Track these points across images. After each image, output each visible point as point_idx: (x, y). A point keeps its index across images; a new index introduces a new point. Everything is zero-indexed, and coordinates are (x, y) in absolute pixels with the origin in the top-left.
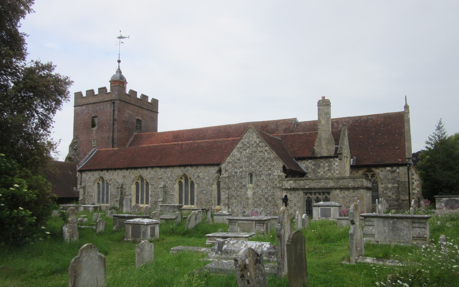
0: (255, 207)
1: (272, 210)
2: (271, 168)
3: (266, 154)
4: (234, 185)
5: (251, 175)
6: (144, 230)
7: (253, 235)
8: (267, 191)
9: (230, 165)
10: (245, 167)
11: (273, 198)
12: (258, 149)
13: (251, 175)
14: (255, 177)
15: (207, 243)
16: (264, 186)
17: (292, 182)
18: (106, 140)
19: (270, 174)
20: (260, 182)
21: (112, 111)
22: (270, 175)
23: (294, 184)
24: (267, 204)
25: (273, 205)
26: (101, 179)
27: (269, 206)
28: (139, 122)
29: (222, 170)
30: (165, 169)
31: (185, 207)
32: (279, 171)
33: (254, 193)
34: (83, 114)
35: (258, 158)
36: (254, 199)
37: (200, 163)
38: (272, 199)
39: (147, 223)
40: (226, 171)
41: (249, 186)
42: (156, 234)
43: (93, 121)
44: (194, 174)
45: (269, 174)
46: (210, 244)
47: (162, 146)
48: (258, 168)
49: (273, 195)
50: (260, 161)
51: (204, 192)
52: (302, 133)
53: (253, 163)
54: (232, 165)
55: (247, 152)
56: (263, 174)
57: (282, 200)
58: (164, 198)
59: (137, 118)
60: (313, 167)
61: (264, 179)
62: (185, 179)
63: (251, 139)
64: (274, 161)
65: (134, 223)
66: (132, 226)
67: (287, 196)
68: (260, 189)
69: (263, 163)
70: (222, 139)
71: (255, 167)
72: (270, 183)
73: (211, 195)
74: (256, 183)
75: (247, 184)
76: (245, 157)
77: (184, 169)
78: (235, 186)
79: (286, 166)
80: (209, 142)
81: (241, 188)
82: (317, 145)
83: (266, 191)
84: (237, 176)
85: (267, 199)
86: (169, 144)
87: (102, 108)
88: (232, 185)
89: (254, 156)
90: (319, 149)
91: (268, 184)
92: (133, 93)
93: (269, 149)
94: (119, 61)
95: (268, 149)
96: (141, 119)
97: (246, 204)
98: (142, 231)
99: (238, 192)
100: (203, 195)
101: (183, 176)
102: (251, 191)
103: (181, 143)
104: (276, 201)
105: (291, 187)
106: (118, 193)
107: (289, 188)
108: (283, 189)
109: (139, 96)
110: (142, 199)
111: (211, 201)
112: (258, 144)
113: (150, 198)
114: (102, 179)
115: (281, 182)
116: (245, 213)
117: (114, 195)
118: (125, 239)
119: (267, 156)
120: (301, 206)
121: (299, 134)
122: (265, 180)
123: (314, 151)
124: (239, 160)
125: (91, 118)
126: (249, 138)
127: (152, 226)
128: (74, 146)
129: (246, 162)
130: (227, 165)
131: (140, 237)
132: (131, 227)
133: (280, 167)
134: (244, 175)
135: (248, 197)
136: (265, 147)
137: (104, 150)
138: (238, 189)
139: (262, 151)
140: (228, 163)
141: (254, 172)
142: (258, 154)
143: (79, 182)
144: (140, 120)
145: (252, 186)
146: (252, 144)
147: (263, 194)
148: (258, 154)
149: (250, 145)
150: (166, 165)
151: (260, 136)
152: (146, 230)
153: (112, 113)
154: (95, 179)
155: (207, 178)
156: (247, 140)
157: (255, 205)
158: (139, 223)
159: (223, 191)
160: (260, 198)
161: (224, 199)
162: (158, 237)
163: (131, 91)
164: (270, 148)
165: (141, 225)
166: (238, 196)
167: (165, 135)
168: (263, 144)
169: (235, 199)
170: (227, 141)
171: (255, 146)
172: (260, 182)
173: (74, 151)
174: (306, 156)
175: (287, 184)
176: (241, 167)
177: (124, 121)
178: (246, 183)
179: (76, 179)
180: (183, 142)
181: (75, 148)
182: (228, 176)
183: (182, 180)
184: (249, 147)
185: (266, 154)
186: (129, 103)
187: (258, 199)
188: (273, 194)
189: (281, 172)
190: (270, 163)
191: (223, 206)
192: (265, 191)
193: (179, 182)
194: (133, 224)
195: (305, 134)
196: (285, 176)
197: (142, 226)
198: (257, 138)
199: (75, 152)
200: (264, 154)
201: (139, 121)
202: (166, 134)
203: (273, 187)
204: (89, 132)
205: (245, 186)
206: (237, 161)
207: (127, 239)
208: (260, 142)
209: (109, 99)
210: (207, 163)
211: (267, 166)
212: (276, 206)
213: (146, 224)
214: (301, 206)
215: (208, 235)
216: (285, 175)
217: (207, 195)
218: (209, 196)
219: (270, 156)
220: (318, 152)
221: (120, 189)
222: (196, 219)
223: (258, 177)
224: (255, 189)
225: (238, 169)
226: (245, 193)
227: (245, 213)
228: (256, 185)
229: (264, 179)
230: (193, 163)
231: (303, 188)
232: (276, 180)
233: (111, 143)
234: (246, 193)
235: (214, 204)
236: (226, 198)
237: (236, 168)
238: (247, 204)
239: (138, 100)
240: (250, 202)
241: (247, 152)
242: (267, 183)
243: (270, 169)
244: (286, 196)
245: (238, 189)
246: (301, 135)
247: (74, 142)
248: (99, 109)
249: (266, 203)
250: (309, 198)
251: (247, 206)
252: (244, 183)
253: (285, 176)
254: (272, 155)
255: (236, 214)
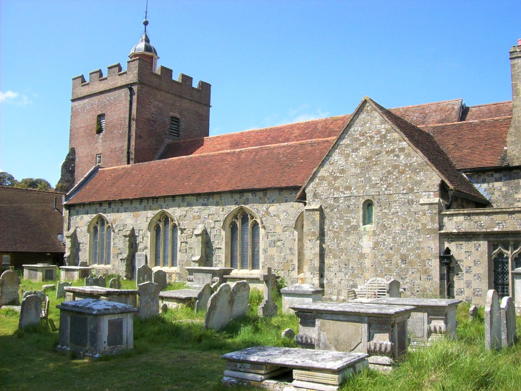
0: (377, 276)
1: (417, 282)
2: (413, 187)
3: (402, 157)
4: (334, 227)
5: (368, 205)
6: (92, 328)
7: (356, 362)
8: (405, 240)
9: (325, 183)
10: (357, 187)
11: (419, 256)
12: (385, 146)
13: (368, 205)
14: (379, 209)
15: (225, 379)
16: (397, 229)
17: (461, 218)
18: (117, 153)
19: (412, 201)
20: (388, 219)
21: (128, 103)
22: (410, 202)
23: (467, 223)
24: (405, 269)
25: (418, 271)
26: (99, 220)
27: (410, 272)
28: (176, 122)
29: (308, 195)
30: (206, 200)
31: (236, 272)
32: (432, 193)
33: (376, 244)
34: (83, 112)
35: (384, 167)
36: (375, 257)
37: (270, 186)
38: (416, 257)
39: (98, 310)
40: (315, 195)
41: (365, 229)
42: (125, 337)
43: (99, 123)
44: (259, 209)
45: (408, 201)
46: (234, 380)
47: (205, 156)
48: (383, 189)
49: (418, 249)
50: (389, 173)
51: (279, 243)
52: (477, 121)
53: (373, 178)
54: (329, 185)
55: (360, 153)
56: (395, 201)
57: (438, 260)
58: (204, 255)
59: (172, 114)
60: (504, 189)
61: (397, 212)
62: (242, 219)
63: (368, 125)
64: (419, 172)
65: (76, 309)
66: (71, 316)
67: (450, 251)
68: (389, 235)
69: (394, 177)
70: (316, 140)
71: (379, 187)
72: (411, 221)
73: (291, 249)
74: (381, 221)
75: (361, 224)
76: (356, 165)
77: (240, 198)
78: (335, 229)
79: (447, 182)
80: (291, 146)
81: (348, 233)
82: (512, 142)
83: (403, 239)
84: (339, 206)
85: (404, 259)
86: (217, 152)
87: (112, 100)
88: (329, 227)
89: (376, 162)
90: (517, 150)
91: (407, 224)
92: (167, 72)
93: (409, 145)
94: (146, 23)
95: (407, 146)
96: (178, 116)
97: (358, 267)
98: (89, 330)
99: (342, 241)
100: (275, 248)
101: (239, 213)
102: (369, 240)
103: (239, 150)
104: (424, 261)
105: (459, 229)
106: (125, 245)
107: (455, 231)
108: (441, 235)
109: (176, 77)
110: (165, 257)
111: (292, 261)
112: (385, 136)
113: (179, 254)
114: (101, 220)
115: (437, 218)
116: (357, 288)
117: (119, 249)
118: (59, 346)
119: (403, 162)
120: (482, 272)
121: (472, 123)
122: (399, 214)
123: (505, 155)
124: (342, 171)
125: (96, 117)
126: (365, 123)
127: (116, 317)
128: (70, 166)
129: (357, 175)
130: (317, 184)
131: (85, 345)
132: (69, 319)
133: (434, 185)
134: (354, 204)
135: (364, 252)
136: (400, 141)
137: (109, 170)
138: (342, 235)
139: (393, 151)
140: (319, 179)
141: (376, 197)
142: (384, 158)
143: (66, 226)
144: (177, 119)
145: (371, 228)
146: (371, 137)
147: (396, 245)
148: (384, 158)
149: (367, 139)
150: (207, 190)
151: (389, 119)
152: (97, 328)
153: (128, 106)
154: (91, 220)
155: (282, 216)
156: (360, 129)
157: (379, 271)
158: (83, 311)
159: (310, 240)
160: (389, 254)
161: (311, 258)
162: (132, 347)
163: (163, 68)
164: (409, 142)
165: (87, 316)
166: (342, 250)
167: (217, 141)
168: (396, 135)
169: (335, 257)
170: (324, 142)
171: (378, 141)
172: (388, 219)
173: (70, 175)
174: (489, 165)
175: (450, 222)
176: (348, 188)
177: (149, 120)
178: (358, 222)
179: (62, 219)
180: (241, 149)
181: (70, 169)
182: (321, 207)
183: (236, 220)
184: (363, 144)
185: (402, 157)
186: (157, 89)
187: (384, 257)
188: (418, 245)
189: (435, 196)
190: (410, 177)
191: (309, 271)
192: (400, 239)
193: (230, 224)
194: (72, 311)
195: (483, 122)
196: (446, 205)
197: (90, 318)
198: (382, 123)
199: (71, 177)
200: (398, 156)
201: (175, 120)
202: (219, 140)
203: (418, 231)
204: (92, 142)
205: (355, 228)
206: (338, 175)
207: (62, 345)
208: (388, 131)
209: (123, 84)
210: (284, 185)
211: (404, 184)
212: (426, 272)
213: (95, 312)
214: (482, 272)
215: (228, 355)
216: (446, 203)
217: (284, 249)
218: (288, 252)
219: (410, 160)
220: (515, 155)
221: (128, 239)
222: (231, 302)
223: (385, 208)
224: (379, 234)
225: (342, 192)
226: (355, 243)
227: (357, 288)
228: (379, 225)
229: (397, 212)
230: (256, 187)
231: (489, 230)
232: (425, 215)
233: (125, 159)
234: (359, 244)
235: (296, 267)
236: (315, 254)
237: (337, 189)
238: (362, 269)
239: (174, 83)
240: (367, 263)
241: (360, 153)
242: (406, 220)
243: (411, 190)
244: (448, 251)
245: (342, 235)
246: (476, 125)
247: (69, 159)
248: (108, 101)
249: (403, 266)
250: (501, 254)
251: (360, 272)
252: (354, 223)
253: (446, 205)
254: (415, 158)
255: (336, 291)
